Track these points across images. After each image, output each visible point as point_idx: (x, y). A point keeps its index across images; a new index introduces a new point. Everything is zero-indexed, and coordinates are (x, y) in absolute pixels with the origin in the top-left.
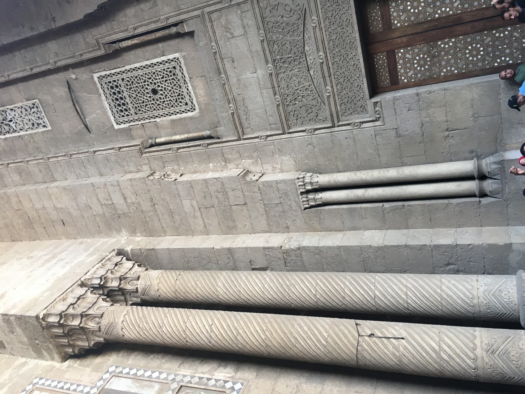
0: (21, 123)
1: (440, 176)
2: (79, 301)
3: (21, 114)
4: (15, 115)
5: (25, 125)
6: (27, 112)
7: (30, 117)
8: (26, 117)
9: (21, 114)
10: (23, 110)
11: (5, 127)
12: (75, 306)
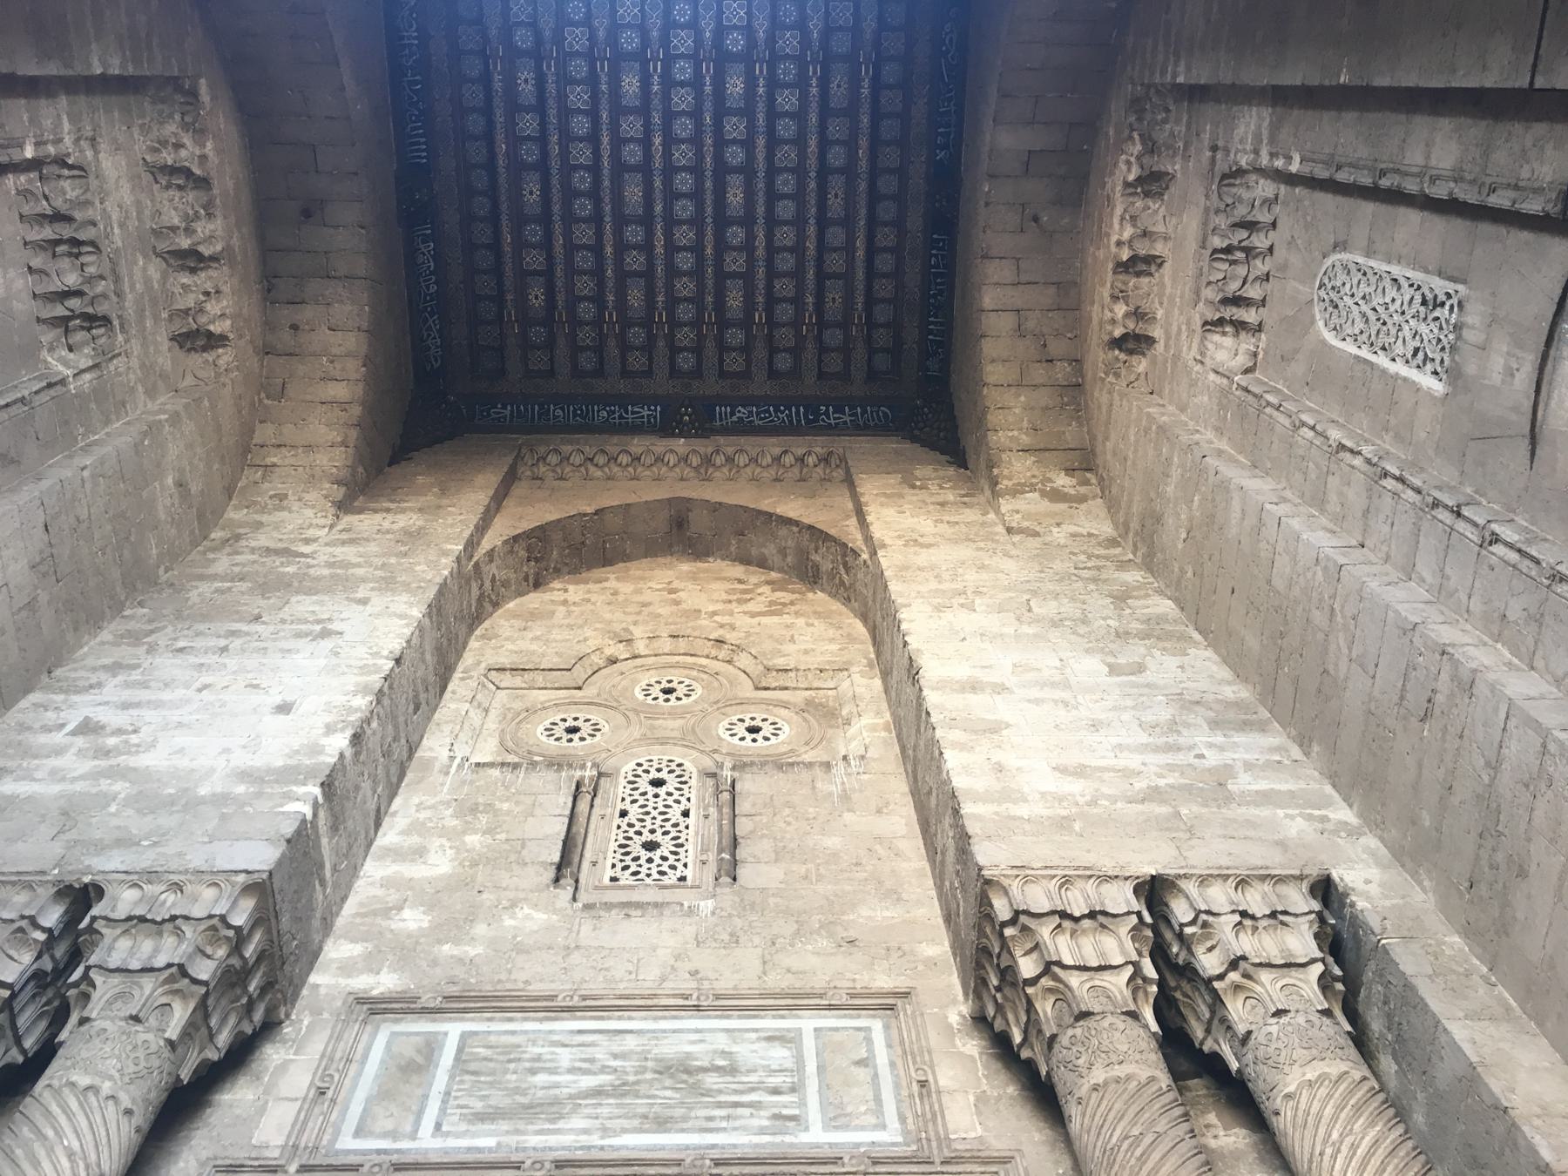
0: (1393, 331)
2: (1086, 923)
3: (1405, 307)
5: (1400, 341)
6: (1422, 309)
7: (1423, 329)
9: (1405, 307)
10: (1418, 299)
11: (1358, 320)
12: (1067, 924)
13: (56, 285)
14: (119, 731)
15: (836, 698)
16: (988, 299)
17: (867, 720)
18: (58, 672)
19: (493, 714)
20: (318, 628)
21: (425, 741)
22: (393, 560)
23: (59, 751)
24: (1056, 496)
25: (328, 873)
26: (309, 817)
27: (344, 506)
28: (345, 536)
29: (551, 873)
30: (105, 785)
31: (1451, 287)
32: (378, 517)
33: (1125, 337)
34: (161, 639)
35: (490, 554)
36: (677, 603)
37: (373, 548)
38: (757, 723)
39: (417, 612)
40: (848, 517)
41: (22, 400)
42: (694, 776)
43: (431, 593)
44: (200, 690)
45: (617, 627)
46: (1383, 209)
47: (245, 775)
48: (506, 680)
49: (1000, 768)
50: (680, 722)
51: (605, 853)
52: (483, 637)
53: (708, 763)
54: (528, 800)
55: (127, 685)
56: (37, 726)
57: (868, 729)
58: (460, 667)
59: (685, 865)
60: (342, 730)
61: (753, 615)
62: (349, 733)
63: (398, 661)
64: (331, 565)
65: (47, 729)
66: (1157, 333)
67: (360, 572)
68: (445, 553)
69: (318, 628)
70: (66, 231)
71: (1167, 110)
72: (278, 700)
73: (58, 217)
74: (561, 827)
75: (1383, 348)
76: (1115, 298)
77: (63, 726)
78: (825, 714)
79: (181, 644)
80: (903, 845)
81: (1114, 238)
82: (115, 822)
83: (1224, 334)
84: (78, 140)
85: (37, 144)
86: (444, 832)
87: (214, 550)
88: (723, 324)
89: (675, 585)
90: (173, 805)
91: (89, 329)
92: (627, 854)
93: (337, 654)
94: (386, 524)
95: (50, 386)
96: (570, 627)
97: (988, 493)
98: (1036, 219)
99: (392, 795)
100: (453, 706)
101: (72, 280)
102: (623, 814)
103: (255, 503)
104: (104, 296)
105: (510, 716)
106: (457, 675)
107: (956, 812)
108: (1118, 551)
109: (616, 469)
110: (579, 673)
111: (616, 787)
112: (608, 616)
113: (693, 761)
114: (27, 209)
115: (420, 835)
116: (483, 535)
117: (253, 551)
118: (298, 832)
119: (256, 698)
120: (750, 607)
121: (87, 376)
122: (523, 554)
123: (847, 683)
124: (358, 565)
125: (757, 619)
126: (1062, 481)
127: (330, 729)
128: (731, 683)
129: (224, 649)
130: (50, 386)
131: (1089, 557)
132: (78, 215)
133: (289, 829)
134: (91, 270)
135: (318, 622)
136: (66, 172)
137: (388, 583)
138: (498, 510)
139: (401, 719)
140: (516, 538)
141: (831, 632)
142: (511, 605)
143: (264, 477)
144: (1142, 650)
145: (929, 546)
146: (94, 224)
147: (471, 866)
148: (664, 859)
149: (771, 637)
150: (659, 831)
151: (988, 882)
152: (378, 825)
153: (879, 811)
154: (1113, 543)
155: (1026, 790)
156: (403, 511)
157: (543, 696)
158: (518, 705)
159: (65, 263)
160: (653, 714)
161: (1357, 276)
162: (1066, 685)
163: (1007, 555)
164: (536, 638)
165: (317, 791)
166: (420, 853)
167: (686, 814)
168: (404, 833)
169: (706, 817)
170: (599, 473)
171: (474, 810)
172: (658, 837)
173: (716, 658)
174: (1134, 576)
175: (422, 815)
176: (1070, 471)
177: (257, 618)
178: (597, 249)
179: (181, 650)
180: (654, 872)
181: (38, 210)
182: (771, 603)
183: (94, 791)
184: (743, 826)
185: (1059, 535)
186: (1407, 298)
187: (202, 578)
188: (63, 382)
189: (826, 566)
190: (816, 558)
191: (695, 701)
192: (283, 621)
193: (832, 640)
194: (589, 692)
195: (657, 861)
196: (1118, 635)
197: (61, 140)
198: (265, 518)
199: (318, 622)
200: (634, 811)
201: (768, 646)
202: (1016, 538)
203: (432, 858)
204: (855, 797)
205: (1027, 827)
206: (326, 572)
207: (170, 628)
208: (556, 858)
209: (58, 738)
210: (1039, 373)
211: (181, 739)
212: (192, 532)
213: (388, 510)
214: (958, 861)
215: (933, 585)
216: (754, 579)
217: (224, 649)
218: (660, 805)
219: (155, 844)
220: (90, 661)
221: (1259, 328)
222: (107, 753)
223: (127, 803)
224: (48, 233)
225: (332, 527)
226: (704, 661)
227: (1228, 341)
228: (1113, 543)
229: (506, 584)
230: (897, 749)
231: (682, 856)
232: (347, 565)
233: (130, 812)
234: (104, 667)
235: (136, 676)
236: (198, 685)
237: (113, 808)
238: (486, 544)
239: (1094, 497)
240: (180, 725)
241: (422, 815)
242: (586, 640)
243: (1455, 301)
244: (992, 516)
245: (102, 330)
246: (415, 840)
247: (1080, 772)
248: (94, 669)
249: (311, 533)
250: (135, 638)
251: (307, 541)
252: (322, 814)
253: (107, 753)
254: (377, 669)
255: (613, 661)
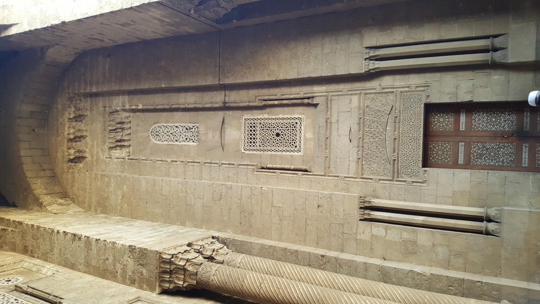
0: (179, 137)
1: (457, 227)
7: (187, 134)
8: (184, 134)
10: (185, 128)
16: (22, 153)
24: (61, 204)
31: (194, 125)
33: (74, 158)
66: (86, 155)
71: (81, 100)
76: (69, 148)
81: (66, 133)
83: (116, 150)
98: (34, 130)
126: (60, 201)
151: (160, 253)
176: (61, 198)
210: (42, 173)
221: (129, 146)
227: (118, 151)
243: (195, 127)
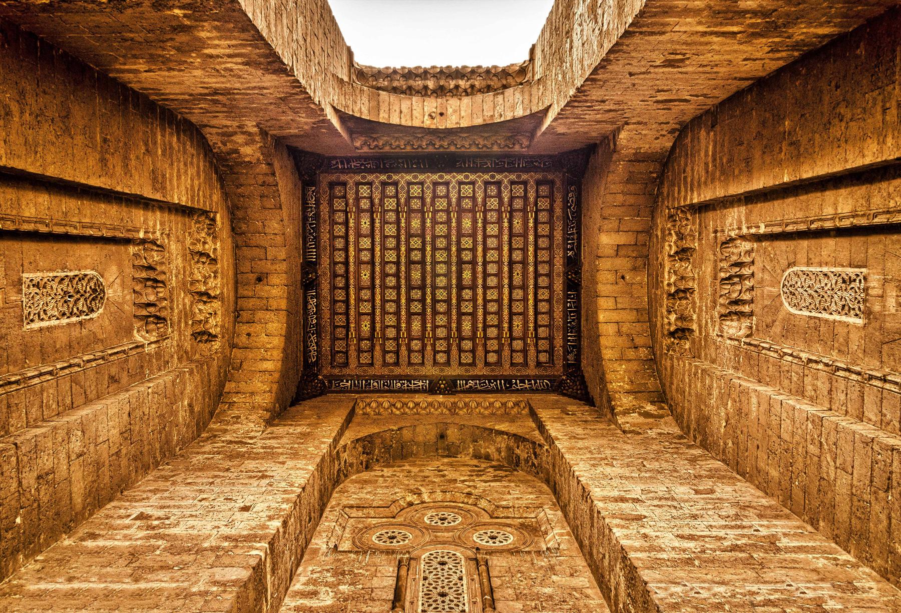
0: (829, 300)
3: (834, 286)
4: (826, 284)
5: (833, 304)
6: (843, 285)
7: (845, 294)
8: (839, 293)
10: (840, 280)
13: (144, 300)
14: (159, 518)
15: (537, 522)
16: (602, 317)
17: (557, 531)
18: (125, 493)
19: (347, 530)
20: (260, 474)
21: (313, 541)
22: (296, 446)
23: (128, 527)
24: (647, 415)
25: (269, 598)
26: (263, 559)
27: (269, 423)
28: (270, 436)
29: (390, 605)
30: (153, 542)
31: (857, 270)
32: (286, 428)
33: (677, 331)
34: (179, 479)
35: (345, 447)
36: (444, 476)
37: (285, 440)
38: (495, 534)
39: (342, 421)
40: (534, 430)
41: (124, 352)
42: (463, 560)
43: (318, 460)
44: (200, 501)
45: (412, 487)
46: (813, 242)
47: (227, 538)
48: (354, 513)
49: (645, 536)
50: (451, 534)
51: (417, 597)
52: (340, 492)
53: (470, 553)
54: (373, 569)
55: (162, 498)
56: (115, 516)
57: (557, 535)
58: (329, 506)
59: (464, 604)
60: (278, 518)
61: (486, 482)
62: (281, 520)
63: (304, 489)
64: (263, 448)
65: (120, 517)
66: (695, 327)
67: (280, 451)
68: (324, 443)
69: (260, 474)
70: (152, 275)
71: (687, 219)
72: (242, 505)
73: (150, 268)
74: (392, 582)
75: (825, 309)
76: (669, 312)
77: (129, 516)
78: (533, 530)
79: (189, 481)
80: (589, 592)
81: (666, 283)
82: (159, 558)
83: (732, 320)
84: (162, 234)
85: (146, 232)
86: (327, 584)
87: (203, 441)
88: (461, 338)
89: (441, 468)
90: (190, 550)
91: (156, 324)
92: (430, 598)
93: (271, 486)
94: (291, 431)
95: (137, 347)
96: (387, 487)
97: (609, 416)
98: (623, 277)
99: (298, 565)
100: (326, 524)
101: (152, 298)
102: (425, 579)
103: (224, 420)
104: (164, 308)
105: (356, 531)
106: (328, 509)
107: (624, 558)
108: (685, 441)
109: (407, 410)
110: (394, 509)
111: (420, 564)
112: (406, 482)
113: (461, 553)
114: (136, 263)
115: (314, 585)
116: (340, 438)
117: (223, 442)
118: (259, 565)
119: (231, 505)
120: (483, 478)
121: (153, 346)
122: (360, 449)
123: (542, 514)
124: (279, 448)
125: (488, 484)
126: (649, 408)
127: (271, 518)
128: (477, 515)
129: (212, 483)
130: (137, 347)
131: (671, 443)
132: (158, 268)
133: (253, 562)
134: (161, 295)
135: (260, 472)
136: (155, 248)
137: (295, 455)
138: (347, 428)
139: (303, 523)
140: (357, 440)
141: (530, 490)
142: (354, 477)
143: (228, 408)
144: (711, 483)
145: (583, 439)
146: (165, 273)
147: (344, 601)
148: (451, 601)
149: (497, 492)
150: (447, 588)
152: (291, 580)
153: (572, 575)
154: (681, 437)
155: (663, 546)
156: (300, 425)
157: (374, 521)
158: (361, 526)
159: (150, 290)
160: (436, 529)
161: (803, 278)
162: (673, 499)
163: (625, 442)
164: (369, 492)
165: (267, 546)
166: (315, 594)
167: (461, 579)
168: (304, 584)
169: (473, 580)
170: (398, 412)
171: (343, 574)
172: (446, 590)
173: (467, 503)
174: (697, 452)
175: (315, 576)
176: (653, 403)
177: (228, 470)
178: (398, 302)
179: (189, 483)
180: (446, 607)
181: (141, 263)
182: (495, 476)
183: (148, 544)
184: (496, 582)
185: (652, 433)
186: (834, 282)
187: (198, 453)
188: (143, 346)
189: (524, 456)
190: (518, 451)
191: (459, 524)
192: (242, 471)
193: (531, 493)
194: (399, 520)
195: (447, 602)
196: (695, 477)
197: (155, 232)
198: (229, 428)
199: (260, 472)
200: (431, 576)
201: (496, 495)
202: (629, 435)
203: (322, 596)
204: (557, 568)
205: (668, 563)
206: (262, 451)
207: (183, 475)
208: (391, 597)
209: (127, 521)
210: (631, 354)
211: (191, 522)
212: (193, 432)
213: (291, 425)
214: (628, 587)
215: (589, 456)
216: (483, 466)
217: (212, 483)
218: (440, 583)
219: (182, 569)
220: (142, 488)
221: (751, 314)
222: (153, 528)
223: (165, 550)
224: (144, 275)
225: (263, 432)
226: (461, 505)
227: (735, 324)
228: (681, 437)
229: (351, 465)
230: (576, 545)
231: (461, 599)
232: (274, 448)
233: (166, 554)
234: (150, 491)
235: (166, 494)
236: (199, 498)
237: (158, 552)
238: (342, 443)
239: (668, 415)
240: (191, 516)
241: (315, 576)
242: (396, 493)
243: (861, 277)
244: (613, 426)
245: (162, 325)
246: (311, 588)
247: (691, 538)
248: (144, 492)
249: (252, 434)
250: (166, 479)
251: (251, 438)
252: (268, 560)
253: (153, 528)
254: (293, 492)
255: (410, 504)
